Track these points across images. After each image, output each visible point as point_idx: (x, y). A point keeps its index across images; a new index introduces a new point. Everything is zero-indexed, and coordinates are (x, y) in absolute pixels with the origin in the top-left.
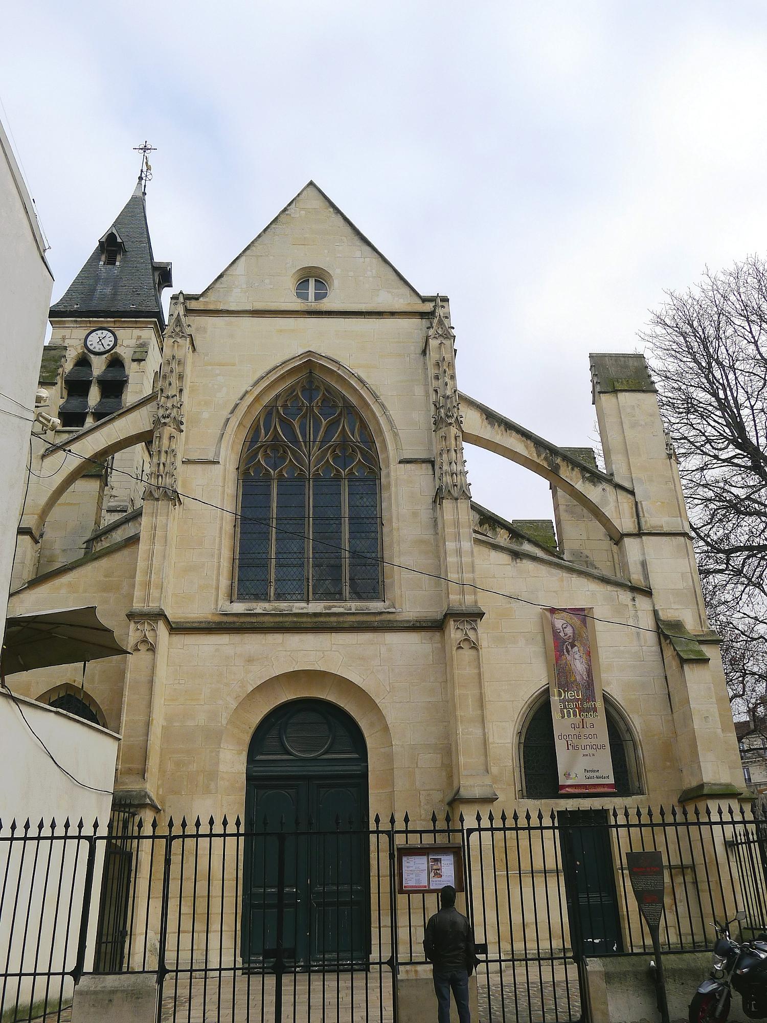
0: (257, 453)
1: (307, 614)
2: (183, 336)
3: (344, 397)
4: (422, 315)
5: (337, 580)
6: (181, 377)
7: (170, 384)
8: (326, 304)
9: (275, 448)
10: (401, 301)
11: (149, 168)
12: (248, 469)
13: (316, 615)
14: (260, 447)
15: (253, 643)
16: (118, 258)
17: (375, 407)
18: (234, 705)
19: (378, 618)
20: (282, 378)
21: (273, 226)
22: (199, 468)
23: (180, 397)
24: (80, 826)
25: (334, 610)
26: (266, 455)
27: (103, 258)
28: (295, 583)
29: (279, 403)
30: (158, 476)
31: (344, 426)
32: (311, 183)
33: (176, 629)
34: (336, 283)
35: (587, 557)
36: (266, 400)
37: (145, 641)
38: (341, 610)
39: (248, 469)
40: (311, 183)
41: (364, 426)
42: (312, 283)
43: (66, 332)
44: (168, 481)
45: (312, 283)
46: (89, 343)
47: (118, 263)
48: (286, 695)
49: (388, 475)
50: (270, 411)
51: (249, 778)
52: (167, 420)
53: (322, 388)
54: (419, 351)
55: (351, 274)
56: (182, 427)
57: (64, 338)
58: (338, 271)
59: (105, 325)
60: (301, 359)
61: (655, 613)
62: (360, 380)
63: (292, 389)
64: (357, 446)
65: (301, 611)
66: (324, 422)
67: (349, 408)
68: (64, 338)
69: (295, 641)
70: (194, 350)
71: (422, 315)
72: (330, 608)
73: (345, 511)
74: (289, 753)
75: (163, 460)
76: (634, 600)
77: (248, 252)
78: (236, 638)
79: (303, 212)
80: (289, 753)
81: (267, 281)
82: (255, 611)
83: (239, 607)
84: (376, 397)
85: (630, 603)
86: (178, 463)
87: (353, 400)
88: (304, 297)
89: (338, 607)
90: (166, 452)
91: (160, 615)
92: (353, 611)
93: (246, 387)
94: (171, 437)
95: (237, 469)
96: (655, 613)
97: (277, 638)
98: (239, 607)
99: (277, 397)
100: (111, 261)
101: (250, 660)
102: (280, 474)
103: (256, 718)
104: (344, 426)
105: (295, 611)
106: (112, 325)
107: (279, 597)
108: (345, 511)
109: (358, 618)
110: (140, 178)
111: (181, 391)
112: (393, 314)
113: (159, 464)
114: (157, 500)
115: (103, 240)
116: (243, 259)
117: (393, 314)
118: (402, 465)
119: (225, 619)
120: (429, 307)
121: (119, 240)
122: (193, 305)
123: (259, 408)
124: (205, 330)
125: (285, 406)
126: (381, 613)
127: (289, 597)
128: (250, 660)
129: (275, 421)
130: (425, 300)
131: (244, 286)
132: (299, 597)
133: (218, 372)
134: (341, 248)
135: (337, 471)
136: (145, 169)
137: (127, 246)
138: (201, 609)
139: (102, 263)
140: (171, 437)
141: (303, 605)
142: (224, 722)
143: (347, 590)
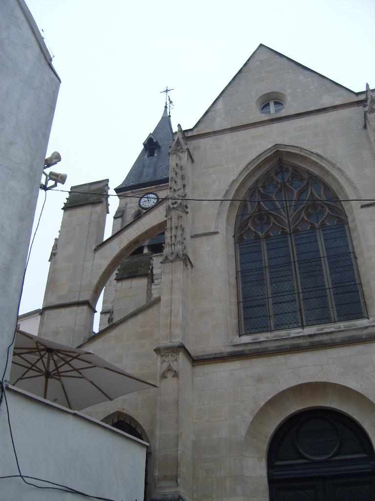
0: (247, 224)
1: (303, 336)
2: (182, 152)
3: (308, 172)
4: (358, 103)
5: (325, 307)
6: (183, 177)
7: (175, 182)
8: (283, 113)
9: (261, 218)
10: (340, 98)
11: (171, 102)
12: (242, 235)
13: (310, 336)
14: (250, 217)
15: (259, 366)
16: (156, 152)
17: (334, 172)
18: (250, 418)
19: (365, 332)
20: (259, 167)
21: (239, 75)
22: (204, 239)
23: (184, 190)
25: (326, 330)
26: (254, 224)
27: (147, 154)
28: (290, 315)
29: (260, 185)
30: (171, 245)
31: (311, 192)
32: (261, 45)
33: (196, 361)
34: (289, 98)
36: (249, 184)
37: (170, 369)
38: (332, 330)
39: (242, 235)
40: (261, 45)
41: (327, 188)
42: (272, 105)
43: (127, 200)
44: (179, 247)
45: (272, 105)
46: (141, 203)
47: (155, 155)
49: (354, 220)
50: (253, 191)
51: (271, 481)
52: (175, 206)
53: (290, 169)
54: (361, 126)
55: (299, 90)
56: (187, 210)
57: (126, 204)
58: (289, 91)
59: (151, 191)
60: (271, 151)
62: (318, 155)
64: (326, 204)
65: (298, 335)
66: (296, 192)
67: (313, 178)
68: (126, 204)
69: (295, 359)
70: (193, 161)
71: (358, 103)
72: (322, 329)
73: (323, 252)
74: (303, 457)
75: (174, 233)
77: (224, 94)
78: (246, 363)
79: (258, 63)
80: (303, 457)
81: (239, 108)
82: (260, 340)
83: (246, 339)
84: (334, 165)
86: (188, 238)
87: (316, 171)
88: (269, 112)
89: (329, 328)
90: (176, 228)
91: (182, 348)
92: (342, 329)
93: (233, 178)
94: (180, 217)
95: (234, 236)
99: (257, 182)
100: (151, 154)
101: (259, 380)
102: (268, 237)
103: (270, 428)
104: (311, 192)
105: (292, 335)
106: (155, 190)
107: (279, 327)
108: (323, 252)
110: (166, 107)
111: (184, 186)
112: (335, 108)
113: (171, 237)
114: (172, 261)
115: (146, 143)
116: (221, 99)
117: (335, 108)
118: (364, 209)
120: (362, 97)
121: (155, 141)
122: (190, 134)
123: (244, 191)
124: (199, 148)
125: (264, 187)
126: (367, 328)
127: (287, 327)
128: (259, 380)
129: (257, 198)
130: (358, 94)
131: (223, 115)
132: (295, 325)
133: (211, 172)
134: (288, 77)
135: (312, 224)
136: (168, 102)
137: (160, 144)
139: (146, 157)
140: (180, 217)
141: (300, 330)
142: (243, 433)
143: (333, 313)
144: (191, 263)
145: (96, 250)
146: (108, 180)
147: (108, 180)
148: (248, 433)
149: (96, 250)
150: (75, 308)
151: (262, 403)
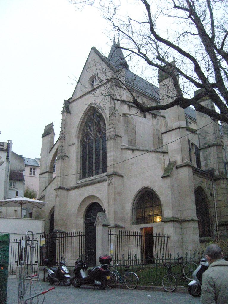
13: (92, 180)
15: (81, 190)
24: (16, 240)
33: (68, 190)
35: (205, 130)
48: (89, 202)
51: (85, 223)
61: (169, 159)
63: (90, 116)
64: (103, 128)
76: (164, 156)
80: (92, 217)
85: (163, 158)
96: (169, 159)
97: (84, 188)
98: (79, 181)
101: (80, 195)
107: (89, 176)
109: (99, 179)
119: (77, 185)
123: (84, 123)
128: (80, 195)
138: (73, 184)
144: (67, 157)
145: (49, 153)
146: (53, 123)
147: (53, 123)
148: (78, 211)
149: (49, 153)
150: (45, 174)
151: (80, 202)
